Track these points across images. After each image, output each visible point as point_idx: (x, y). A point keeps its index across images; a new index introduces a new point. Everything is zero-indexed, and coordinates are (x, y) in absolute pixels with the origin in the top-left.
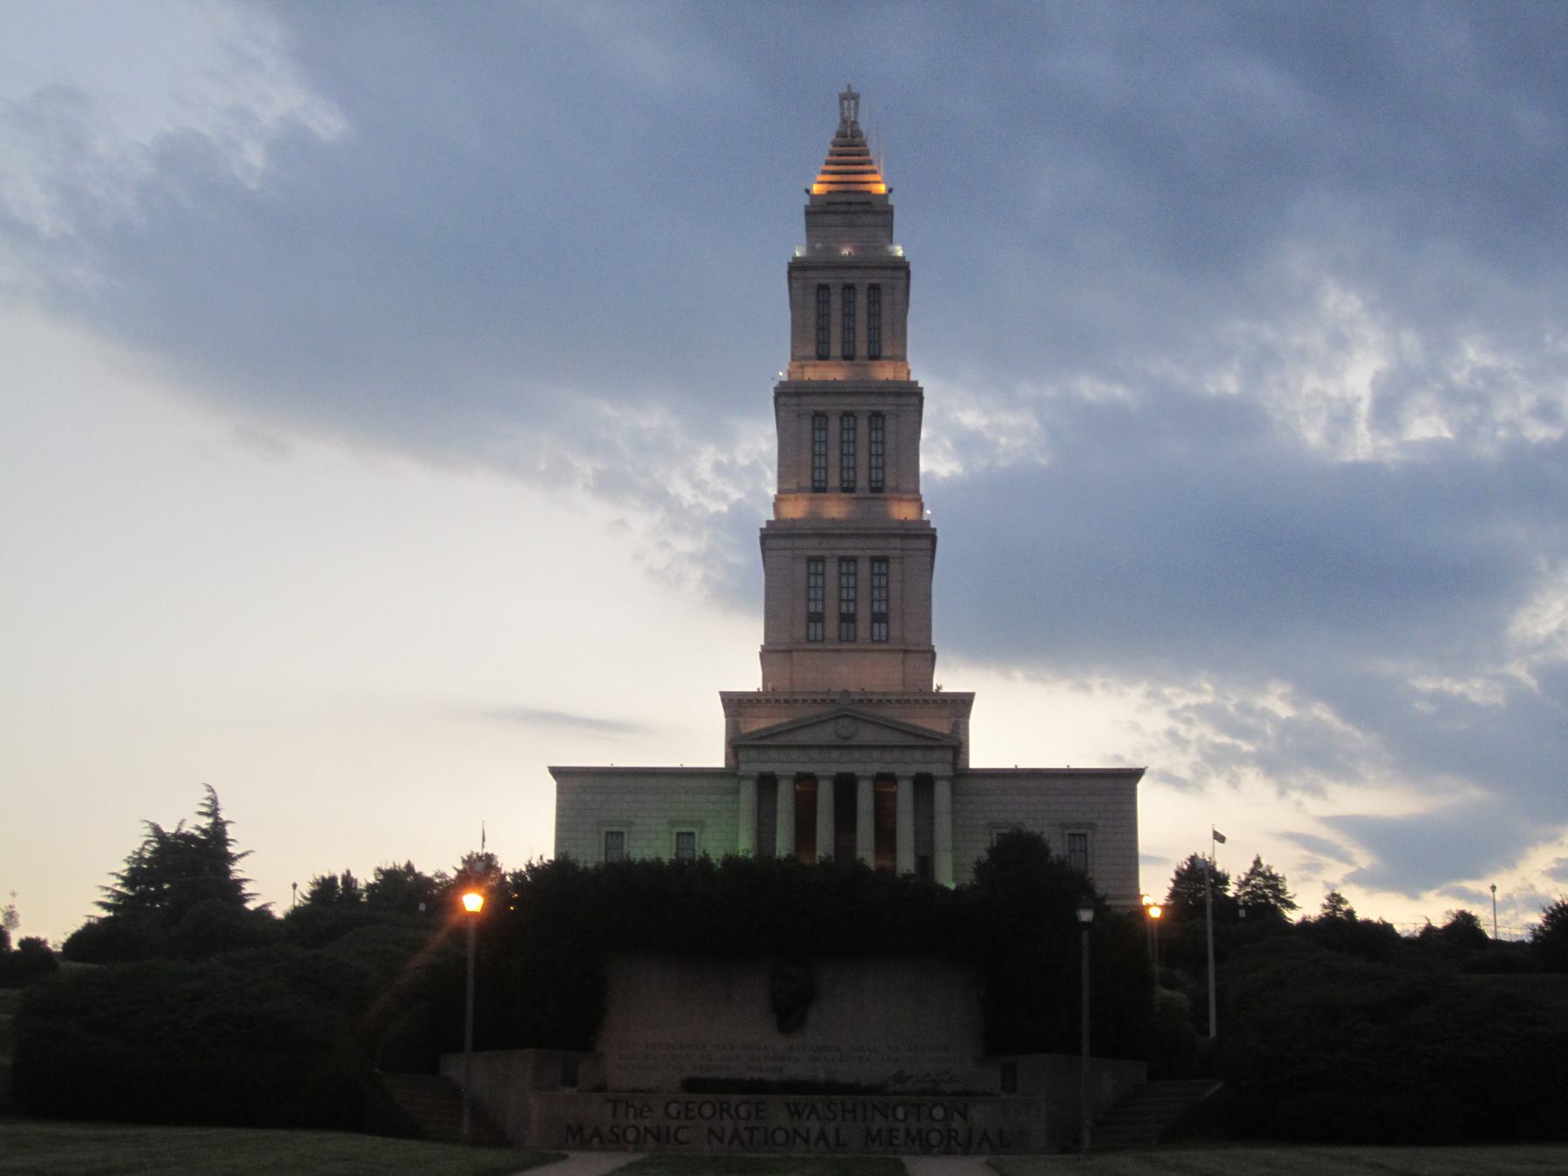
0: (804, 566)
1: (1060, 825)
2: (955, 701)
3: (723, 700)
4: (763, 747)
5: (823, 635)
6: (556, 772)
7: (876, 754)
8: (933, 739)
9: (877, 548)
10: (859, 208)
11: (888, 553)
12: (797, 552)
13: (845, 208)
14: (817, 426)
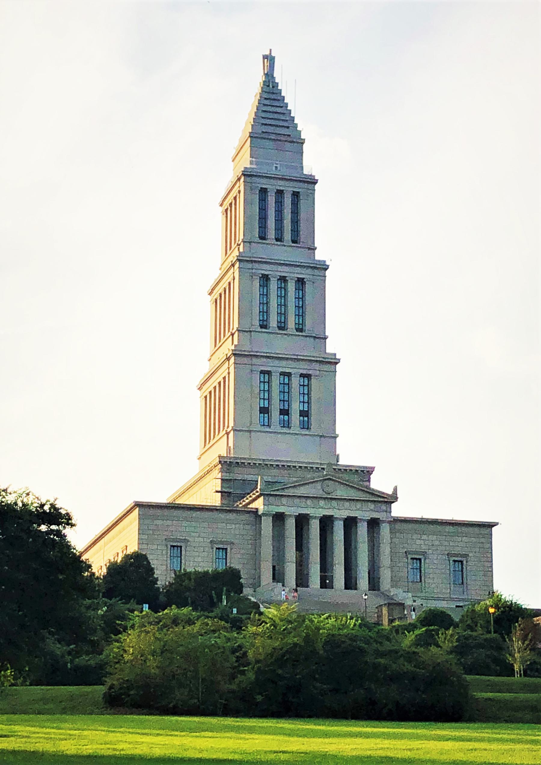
8: (383, 497)
9: (303, 368)
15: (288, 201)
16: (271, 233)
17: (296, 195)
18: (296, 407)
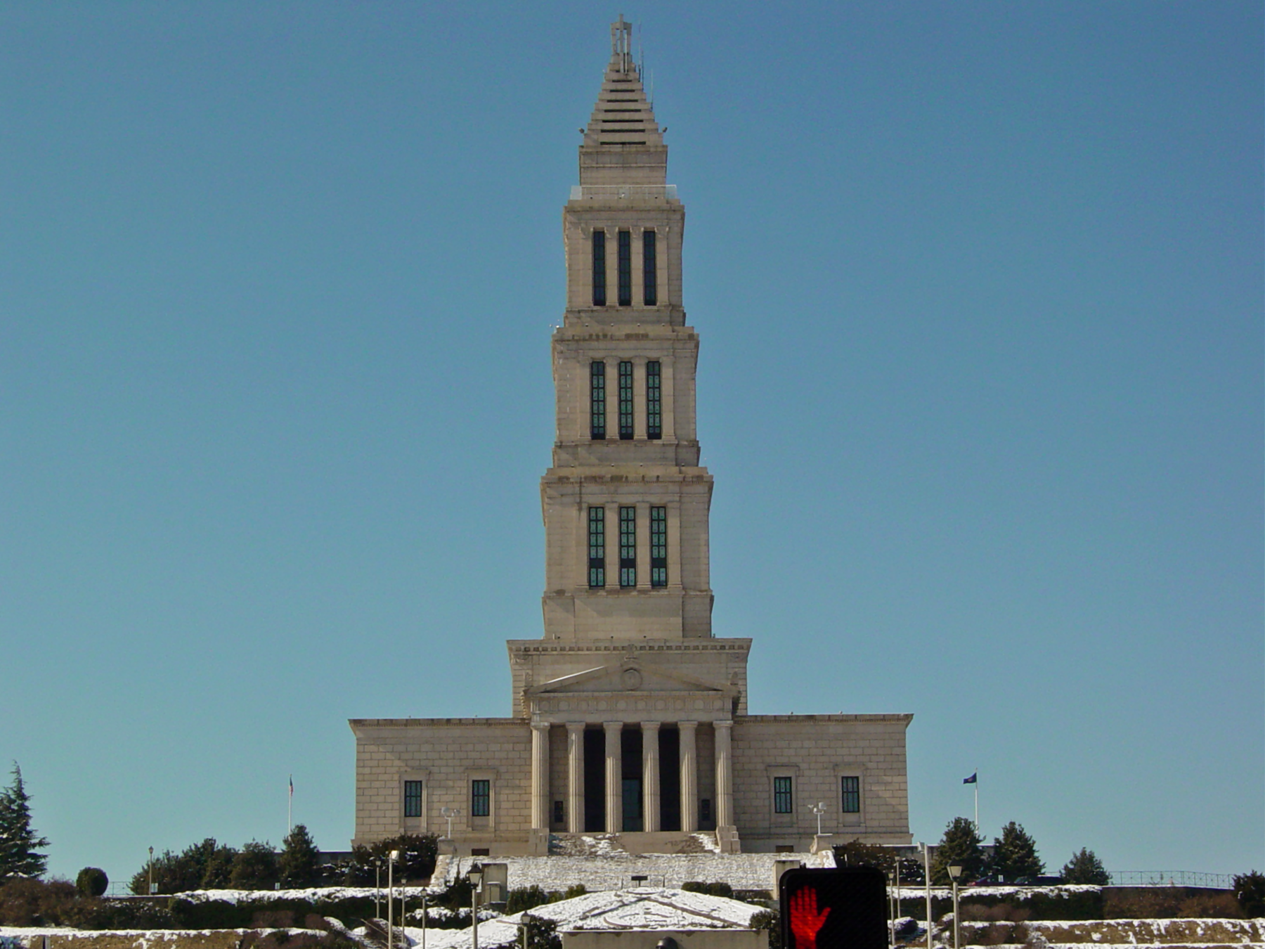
3: (510, 649)
13: (618, 148)
15: (637, 247)
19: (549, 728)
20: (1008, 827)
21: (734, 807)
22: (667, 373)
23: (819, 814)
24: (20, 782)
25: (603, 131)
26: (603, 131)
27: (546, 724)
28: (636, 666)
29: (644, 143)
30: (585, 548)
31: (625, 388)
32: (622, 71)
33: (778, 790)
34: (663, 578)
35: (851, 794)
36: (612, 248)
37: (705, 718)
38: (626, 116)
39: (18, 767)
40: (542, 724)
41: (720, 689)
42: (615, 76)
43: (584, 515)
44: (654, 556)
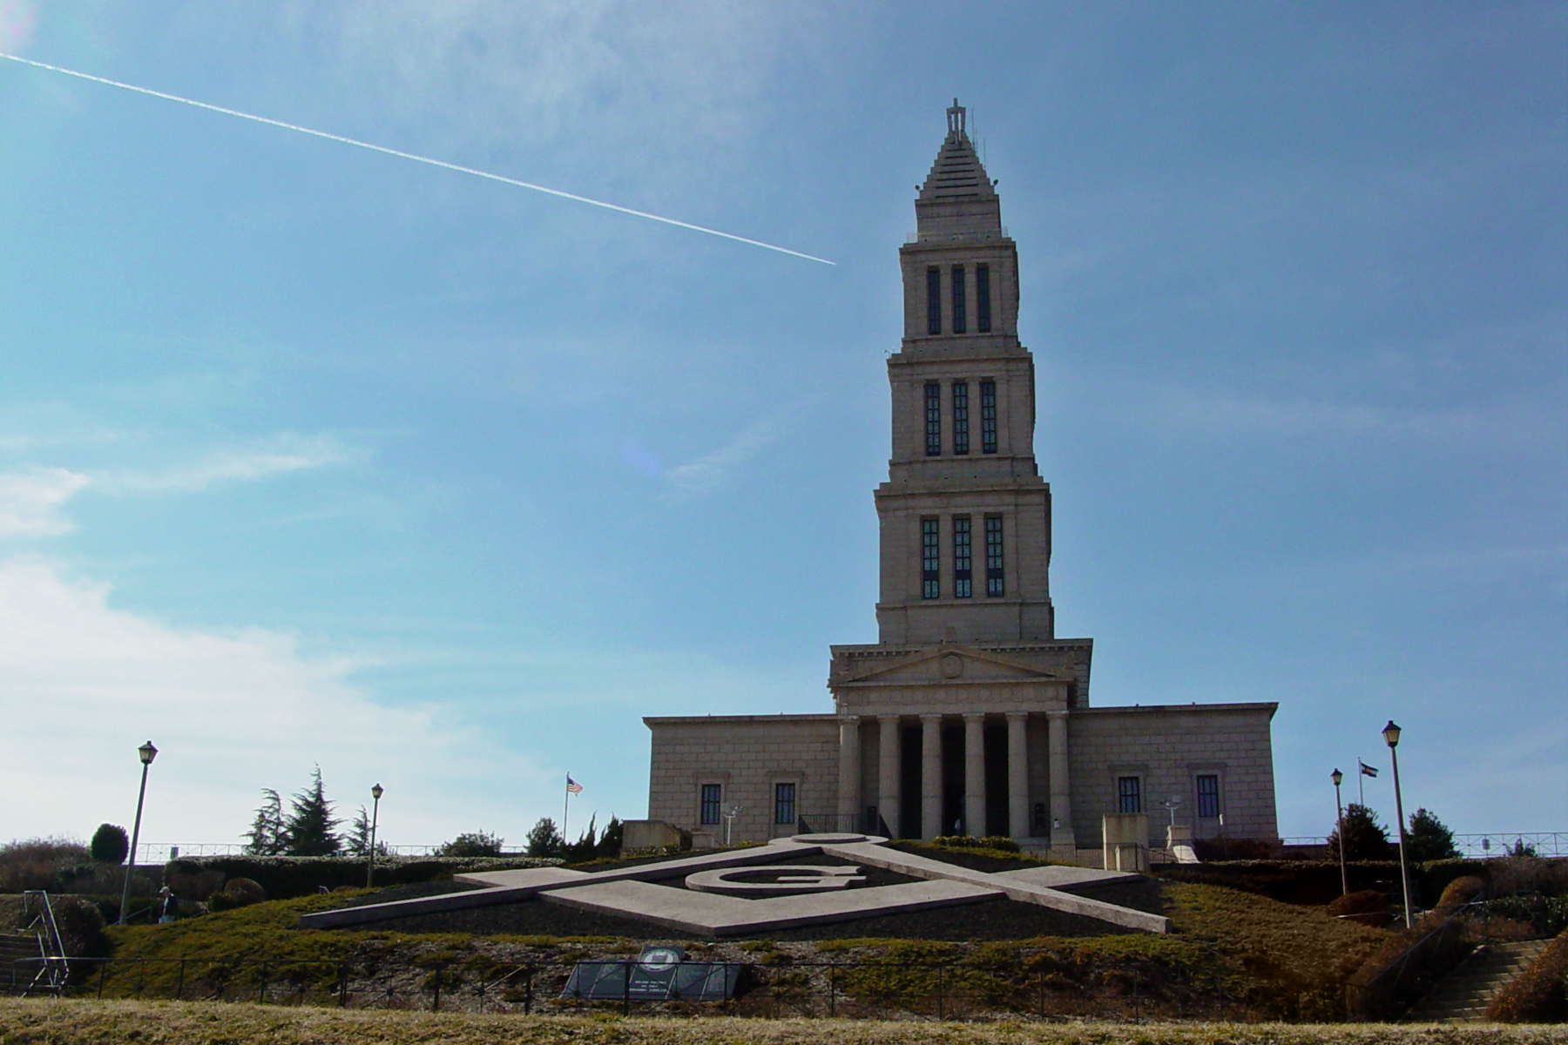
0: (918, 524)
1: (1188, 766)
2: (1071, 648)
4: (858, 688)
5: (939, 592)
6: (649, 722)
7: (985, 693)
9: (991, 504)
10: (967, 199)
11: (1001, 509)
12: (911, 511)
13: (952, 200)
14: (930, 394)
15: (970, 280)
16: (947, 324)
17: (982, 271)
18: (979, 567)
19: (859, 723)
20: (1417, 816)
21: (1072, 811)
22: (1001, 389)
23: (1172, 809)
24: (320, 785)
25: (938, 188)
26: (938, 188)
27: (855, 717)
28: (956, 651)
29: (976, 195)
30: (918, 560)
31: (960, 410)
32: (956, 143)
33: (1123, 793)
34: (1000, 588)
35: (1207, 793)
36: (946, 282)
37: (1035, 707)
38: (960, 175)
39: (319, 770)
40: (850, 717)
41: (1054, 674)
42: (951, 147)
43: (916, 525)
44: (990, 566)
